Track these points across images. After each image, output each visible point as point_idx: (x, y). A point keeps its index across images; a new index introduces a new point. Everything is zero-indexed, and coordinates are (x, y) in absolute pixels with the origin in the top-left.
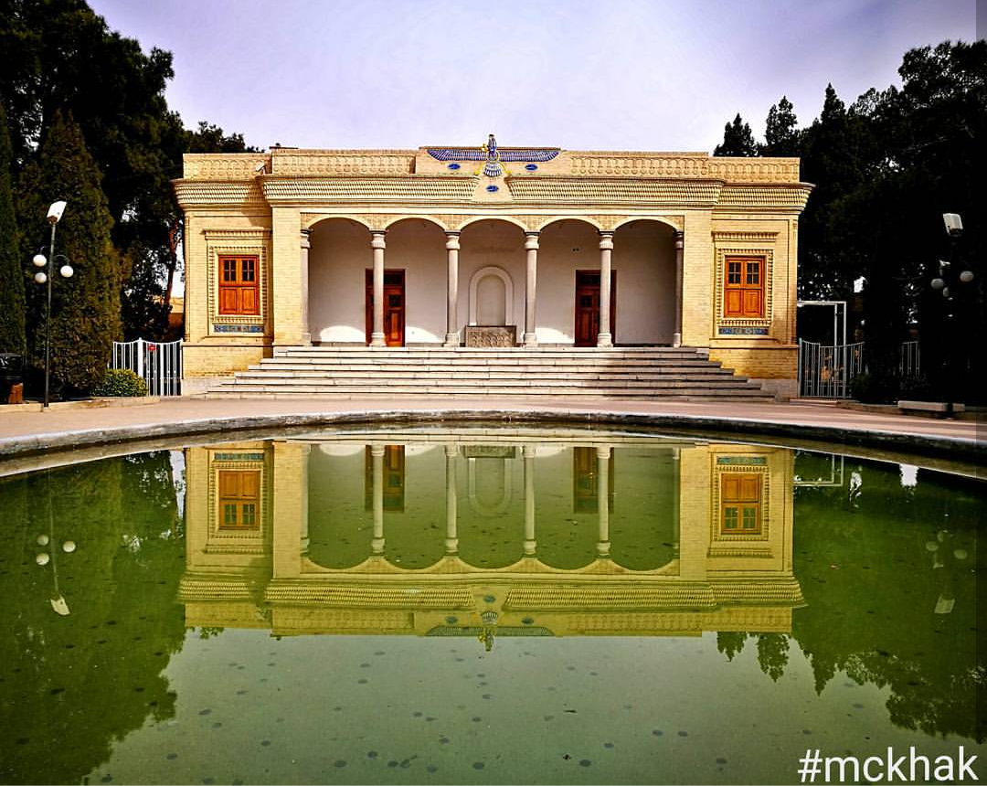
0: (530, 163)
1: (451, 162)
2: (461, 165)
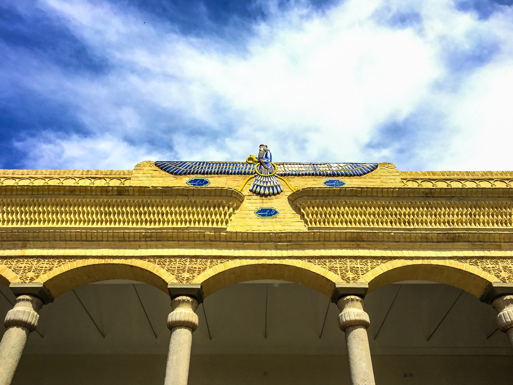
1: (193, 177)
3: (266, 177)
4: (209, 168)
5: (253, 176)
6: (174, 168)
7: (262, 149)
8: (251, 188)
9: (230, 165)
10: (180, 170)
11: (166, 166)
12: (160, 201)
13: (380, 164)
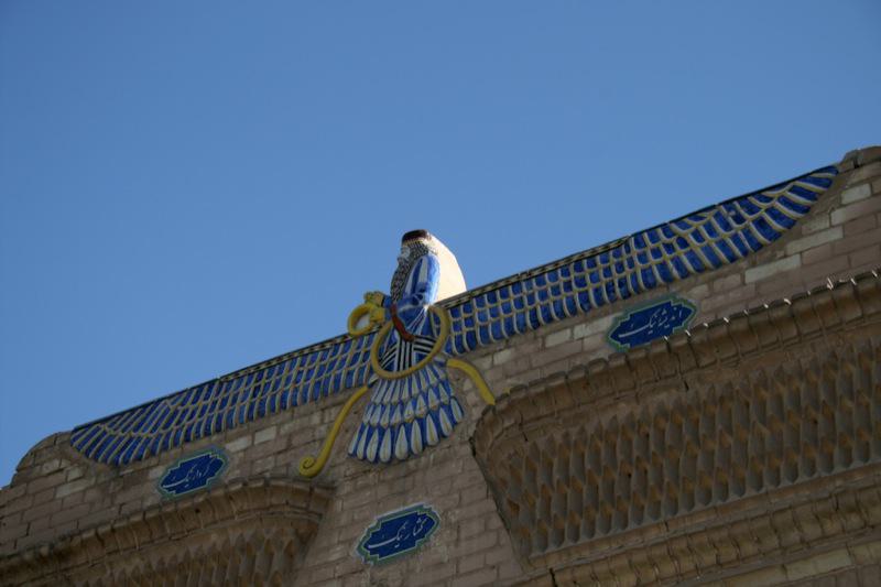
0: (649, 299)
3: (403, 377)
5: (365, 389)
6: (121, 439)
11: (98, 440)
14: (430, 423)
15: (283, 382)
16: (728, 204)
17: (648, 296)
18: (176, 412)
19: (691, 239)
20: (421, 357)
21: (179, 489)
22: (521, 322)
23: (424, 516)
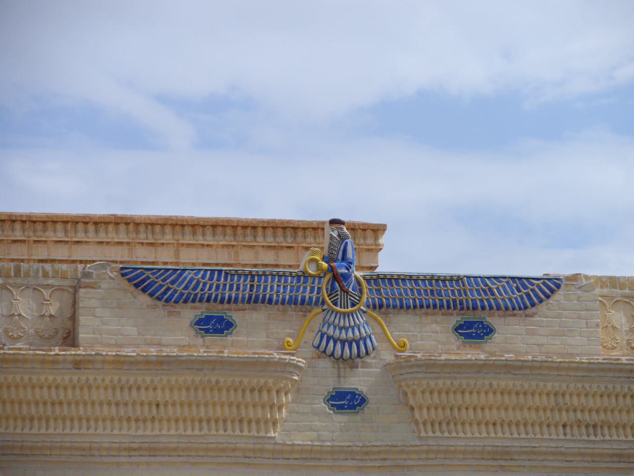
0: (471, 317)
1: (201, 310)
2: (236, 317)
3: (344, 314)
4: (231, 289)
6: (161, 286)
7: (335, 234)
8: (316, 343)
9: (272, 281)
10: (175, 291)
11: (144, 281)
12: (152, 381)
13: (568, 278)
14: (361, 343)
15: (269, 289)
16: (513, 278)
17: (471, 312)
18: (198, 282)
19: (495, 290)
20: (353, 305)
21: (207, 331)
22: (408, 305)
23: (359, 395)
